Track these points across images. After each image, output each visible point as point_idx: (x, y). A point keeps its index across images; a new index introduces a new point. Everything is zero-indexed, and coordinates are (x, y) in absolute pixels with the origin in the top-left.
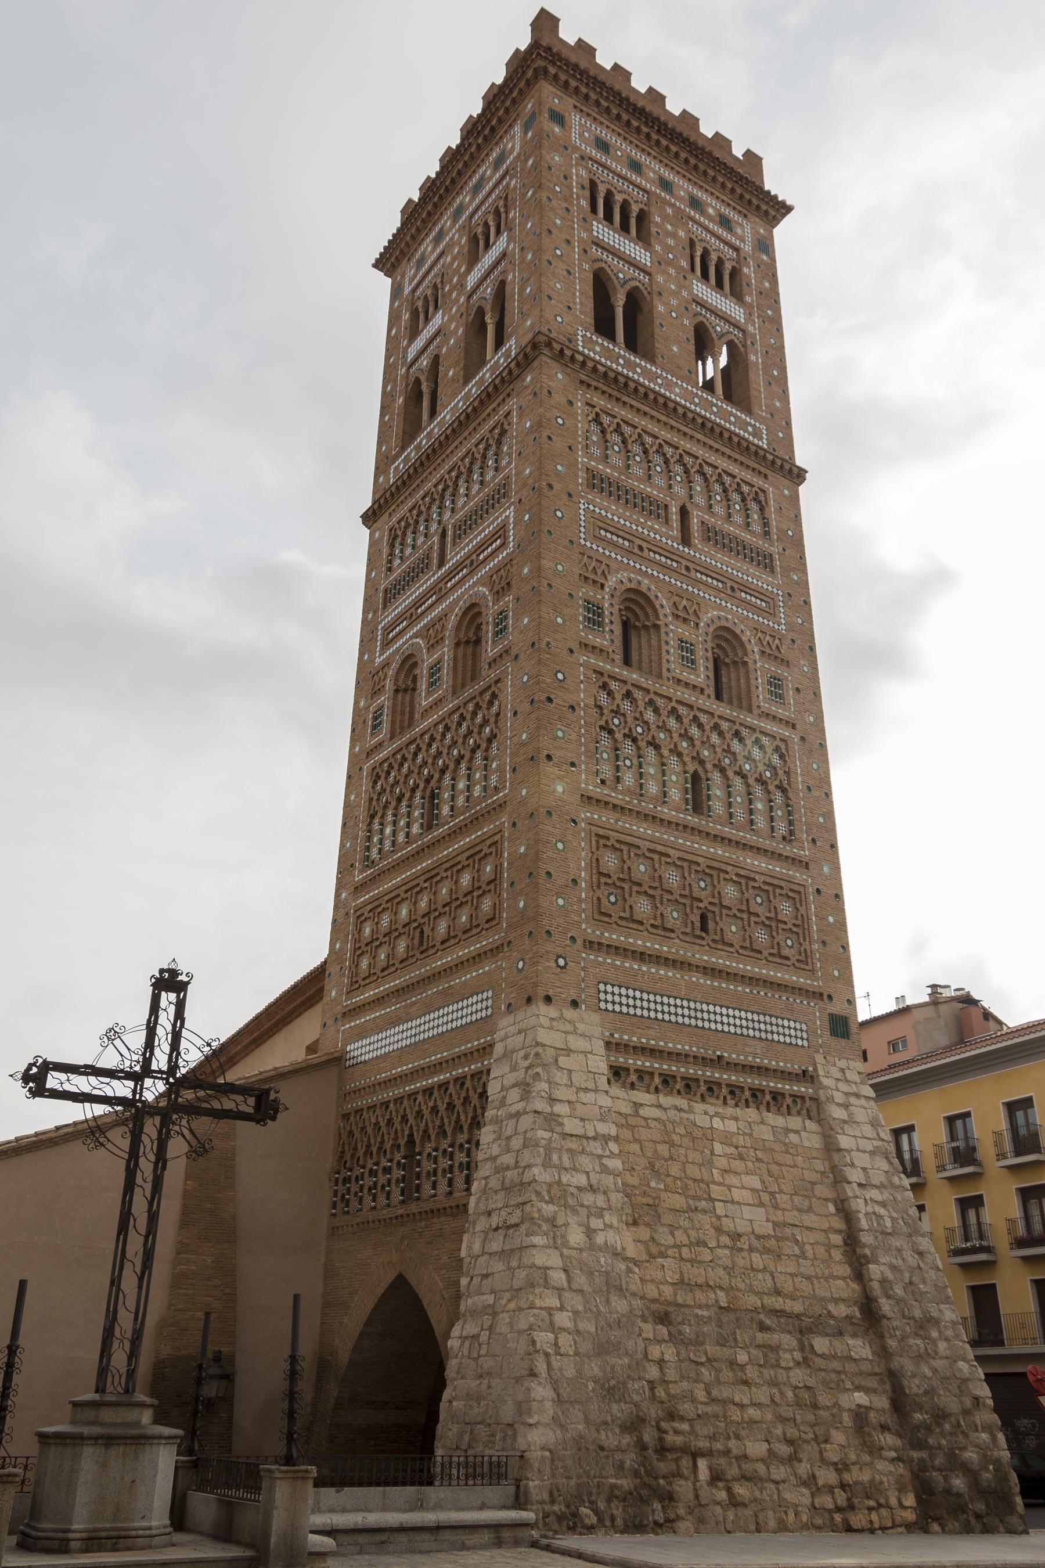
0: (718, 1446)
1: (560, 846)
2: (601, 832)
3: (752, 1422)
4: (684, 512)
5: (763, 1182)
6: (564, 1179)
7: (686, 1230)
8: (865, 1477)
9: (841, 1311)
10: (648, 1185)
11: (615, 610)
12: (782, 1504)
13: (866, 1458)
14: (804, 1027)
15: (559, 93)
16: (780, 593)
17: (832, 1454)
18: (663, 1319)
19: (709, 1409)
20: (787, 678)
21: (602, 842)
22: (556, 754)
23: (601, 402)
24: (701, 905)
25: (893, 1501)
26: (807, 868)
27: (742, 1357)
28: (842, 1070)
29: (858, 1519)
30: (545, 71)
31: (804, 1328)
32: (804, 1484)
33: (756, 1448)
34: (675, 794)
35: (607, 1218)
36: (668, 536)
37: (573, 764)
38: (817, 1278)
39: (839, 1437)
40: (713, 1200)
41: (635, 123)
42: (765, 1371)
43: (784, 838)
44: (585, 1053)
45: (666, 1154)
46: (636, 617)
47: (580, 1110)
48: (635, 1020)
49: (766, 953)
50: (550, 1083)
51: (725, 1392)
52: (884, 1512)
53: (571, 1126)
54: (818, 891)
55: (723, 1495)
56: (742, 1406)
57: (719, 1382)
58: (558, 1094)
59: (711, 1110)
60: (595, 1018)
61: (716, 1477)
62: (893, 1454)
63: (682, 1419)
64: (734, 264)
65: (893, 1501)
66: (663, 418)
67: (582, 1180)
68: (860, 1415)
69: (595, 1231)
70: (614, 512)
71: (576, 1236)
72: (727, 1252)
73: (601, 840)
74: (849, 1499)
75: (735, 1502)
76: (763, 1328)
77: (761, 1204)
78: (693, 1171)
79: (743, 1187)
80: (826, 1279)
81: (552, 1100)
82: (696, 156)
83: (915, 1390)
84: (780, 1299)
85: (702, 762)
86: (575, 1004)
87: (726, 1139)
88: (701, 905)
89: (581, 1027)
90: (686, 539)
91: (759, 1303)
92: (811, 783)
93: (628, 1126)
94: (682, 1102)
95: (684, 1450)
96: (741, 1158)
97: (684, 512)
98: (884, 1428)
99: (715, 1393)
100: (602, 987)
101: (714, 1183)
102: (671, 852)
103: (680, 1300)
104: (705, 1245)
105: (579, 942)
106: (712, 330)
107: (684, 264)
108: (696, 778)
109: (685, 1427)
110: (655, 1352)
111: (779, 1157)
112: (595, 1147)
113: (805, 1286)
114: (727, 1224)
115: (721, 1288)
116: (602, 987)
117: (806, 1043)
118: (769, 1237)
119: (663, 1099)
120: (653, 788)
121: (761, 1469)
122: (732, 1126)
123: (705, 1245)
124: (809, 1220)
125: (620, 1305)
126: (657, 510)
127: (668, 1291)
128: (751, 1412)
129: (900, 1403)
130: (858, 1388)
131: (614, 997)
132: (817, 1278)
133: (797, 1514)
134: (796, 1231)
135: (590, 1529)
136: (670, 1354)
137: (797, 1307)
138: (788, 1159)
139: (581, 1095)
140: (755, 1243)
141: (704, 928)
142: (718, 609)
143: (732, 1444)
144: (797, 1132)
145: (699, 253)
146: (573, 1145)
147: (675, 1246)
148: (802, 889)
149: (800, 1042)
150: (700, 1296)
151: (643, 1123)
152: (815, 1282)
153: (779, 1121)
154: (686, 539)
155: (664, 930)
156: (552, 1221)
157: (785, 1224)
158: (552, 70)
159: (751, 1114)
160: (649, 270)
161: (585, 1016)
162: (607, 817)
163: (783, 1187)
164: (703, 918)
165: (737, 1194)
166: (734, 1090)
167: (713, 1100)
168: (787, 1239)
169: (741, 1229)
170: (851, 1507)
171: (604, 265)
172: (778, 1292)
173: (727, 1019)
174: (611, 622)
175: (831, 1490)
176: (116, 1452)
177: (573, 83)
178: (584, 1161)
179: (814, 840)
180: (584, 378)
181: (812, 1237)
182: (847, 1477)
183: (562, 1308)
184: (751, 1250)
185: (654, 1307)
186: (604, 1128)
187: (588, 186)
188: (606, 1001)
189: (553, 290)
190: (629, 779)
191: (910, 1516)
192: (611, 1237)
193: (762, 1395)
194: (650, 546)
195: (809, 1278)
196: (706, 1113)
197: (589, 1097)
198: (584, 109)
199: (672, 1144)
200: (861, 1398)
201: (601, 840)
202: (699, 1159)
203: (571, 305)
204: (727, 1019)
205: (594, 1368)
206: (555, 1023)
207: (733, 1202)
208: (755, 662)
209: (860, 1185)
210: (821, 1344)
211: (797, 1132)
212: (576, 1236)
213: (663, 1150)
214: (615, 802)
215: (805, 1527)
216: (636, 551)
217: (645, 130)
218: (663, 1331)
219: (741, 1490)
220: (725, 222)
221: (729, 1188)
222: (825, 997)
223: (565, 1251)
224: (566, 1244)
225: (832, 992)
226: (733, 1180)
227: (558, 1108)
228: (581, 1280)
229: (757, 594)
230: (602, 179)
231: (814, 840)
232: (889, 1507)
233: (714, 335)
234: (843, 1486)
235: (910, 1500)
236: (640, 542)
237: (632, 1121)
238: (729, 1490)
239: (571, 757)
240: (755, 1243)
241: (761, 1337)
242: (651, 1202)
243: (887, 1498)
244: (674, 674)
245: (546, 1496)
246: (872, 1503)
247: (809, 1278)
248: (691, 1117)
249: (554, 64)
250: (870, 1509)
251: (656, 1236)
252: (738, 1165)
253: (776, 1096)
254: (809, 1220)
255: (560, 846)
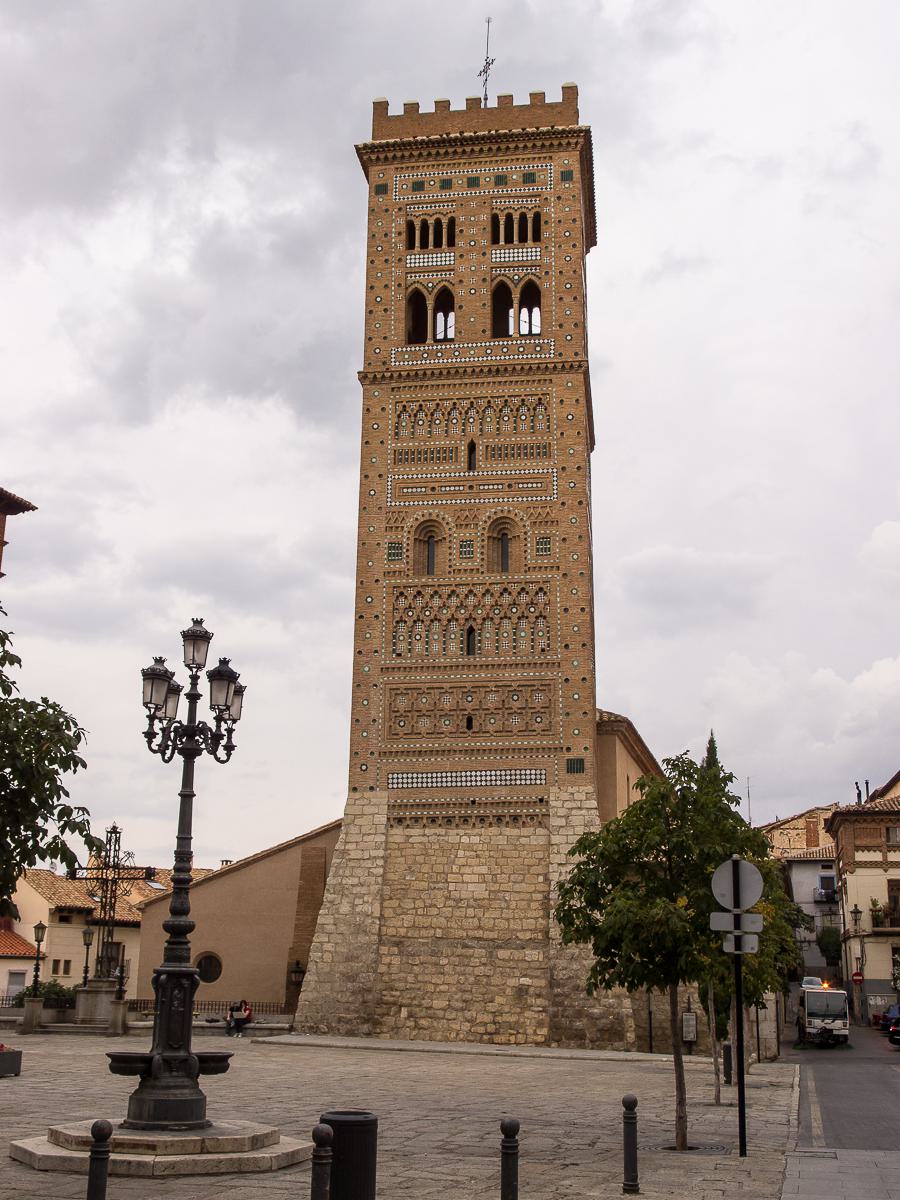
0: (415, 1002)
1: (365, 702)
2: (394, 686)
3: (441, 992)
4: (472, 447)
5: (489, 869)
6: (344, 882)
7: (424, 900)
8: (513, 1019)
9: (528, 935)
10: (404, 879)
11: (411, 542)
12: (450, 1030)
13: (519, 1010)
14: (543, 772)
15: (384, 167)
16: (555, 470)
17: (491, 1007)
18: (397, 944)
19: (413, 986)
20: (554, 534)
21: (393, 692)
22: (364, 650)
23: (405, 396)
24: (466, 713)
25: (530, 1031)
26: (559, 666)
27: (444, 961)
28: (573, 794)
29: (497, 1038)
30: (370, 159)
31: (494, 945)
32: (468, 1021)
33: (439, 1003)
34: (453, 647)
35: (366, 899)
36: (455, 470)
37: (376, 651)
38: (514, 918)
39: (499, 1000)
40: (448, 883)
41: (442, 151)
42: (458, 968)
43: (543, 650)
44: (373, 815)
45: (422, 861)
46: (428, 535)
47: (361, 845)
48: (413, 790)
49: (515, 731)
50: (346, 834)
51: (427, 978)
52: (520, 1036)
53: (353, 855)
54: (567, 680)
55: (412, 1024)
56: (436, 985)
57: (423, 973)
58: (350, 839)
59: (462, 832)
60: (385, 794)
61: (410, 1015)
62: (541, 1009)
63: (396, 990)
64: (537, 209)
65: (530, 1031)
66: (458, 382)
67: (356, 881)
68: (521, 992)
69: (357, 905)
70: (413, 472)
71: (345, 908)
72: (450, 909)
73: (395, 692)
74: (496, 1029)
75: (417, 1027)
76: (465, 946)
77: (484, 882)
78: (440, 868)
79: (473, 874)
80: (521, 919)
81: (346, 843)
82: (496, 142)
83: (561, 976)
84: (481, 932)
85: (475, 619)
86: (372, 788)
87: (469, 847)
88: (466, 713)
89: (374, 801)
90: (471, 466)
91: (465, 934)
92: (568, 605)
93: (399, 849)
94: (442, 831)
95: (394, 1004)
96: (477, 856)
97: (472, 447)
98: (539, 996)
99: (420, 978)
100: (390, 776)
101: (452, 873)
102: (444, 685)
103: (409, 935)
104: (435, 906)
105: (376, 754)
106: (509, 282)
107: (485, 241)
108: (471, 631)
109: (398, 993)
110: (386, 960)
111: (506, 853)
112: (369, 864)
113: (503, 924)
114: (455, 895)
115: (440, 928)
116: (390, 776)
117: (543, 782)
118: (484, 899)
119: (427, 831)
120: (436, 647)
121: (440, 1013)
122: (476, 840)
123: (435, 906)
124: (517, 887)
125: (363, 939)
126: (446, 455)
127: (402, 931)
128: (443, 988)
129: (553, 983)
130: (525, 976)
131: (397, 779)
132: (514, 918)
133: (457, 1034)
134: (507, 894)
135: (325, 1033)
136: (396, 961)
137: (492, 935)
138: (515, 854)
139: (366, 838)
140: (472, 902)
141: (469, 725)
142: (491, 506)
143: (425, 1003)
144: (529, 837)
145: (502, 222)
146: (351, 864)
147: (414, 908)
148: (552, 683)
149: (538, 782)
150: (423, 933)
151: (410, 846)
152: (512, 921)
153: (516, 832)
154: (471, 466)
155: (435, 733)
156: (331, 902)
157: (499, 891)
158: (373, 157)
159: (494, 830)
160: (452, 267)
161: (378, 793)
162: (398, 676)
163: (505, 871)
164: (470, 721)
165: (466, 878)
166: (482, 819)
167: (466, 827)
168: (499, 899)
169: (463, 896)
170: (497, 1032)
171: (416, 285)
172: (480, 928)
173: (480, 778)
174: (407, 550)
175: (485, 1024)
176: (90, 995)
177: (390, 155)
178: (359, 872)
179: (567, 646)
180: (394, 385)
181: (522, 896)
182: (499, 1019)
183: (329, 942)
184: (468, 906)
185: (394, 939)
186: (374, 853)
187: (403, 228)
188: (393, 783)
189: (374, 331)
190: (419, 647)
191: (540, 1039)
192: (367, 908)
193: (452, 980)
194: (440, 484)
195: (508, 920)
196: (458, 835)
197: (371, 838)
198: (403, 166)
199: (427, 855)
200: (525, 981)
201: (395, 692)
202: (445, 860)
203: (388, 334)
204: (480, 778)
205: (341, 968)
206: (357, 802)
207: (463, 882)
208: (525, 533)
209: (560, 864)
210: (502, 954)
211: (529, 837)
212: (345, 908)
213: (420, 859)
214: (404, 665)
215: (461, 1040)
216: (430, 492)
217: (451, 150)
218: (395, 950)
219: (424, 1022)
220: (529, 178)
221: (462, 875)
222: (564, 749)
223: (337, 916)
224: (338, 913)
225: (569, 745)
226: (467, 870)
227: (348, 847)
228: (343, 928)
229: (532, 481)
230: (417, 214)
231: (567, 646)
232: (525, 1033)
233: (511, 286)
234: (494, 1023)
235: (544, 1031)
236: (433, 485)
237: (402, 846)
238: (416, 1022)
239: (375, 647)
240: (472, 902)
241: (459, 951)
242: (404, 887)
243: (526, 1030)
244: (454, 567)
245: (303, 1019)
246: (512, 1032)
247: (508, 920)
248: (446, 838)
249: (372, 152)
250: (511, 1034)
251: (402, 904)
252: (474, 861)
253: (515, 818)
254: (517, 887)
255: (365, 702)
